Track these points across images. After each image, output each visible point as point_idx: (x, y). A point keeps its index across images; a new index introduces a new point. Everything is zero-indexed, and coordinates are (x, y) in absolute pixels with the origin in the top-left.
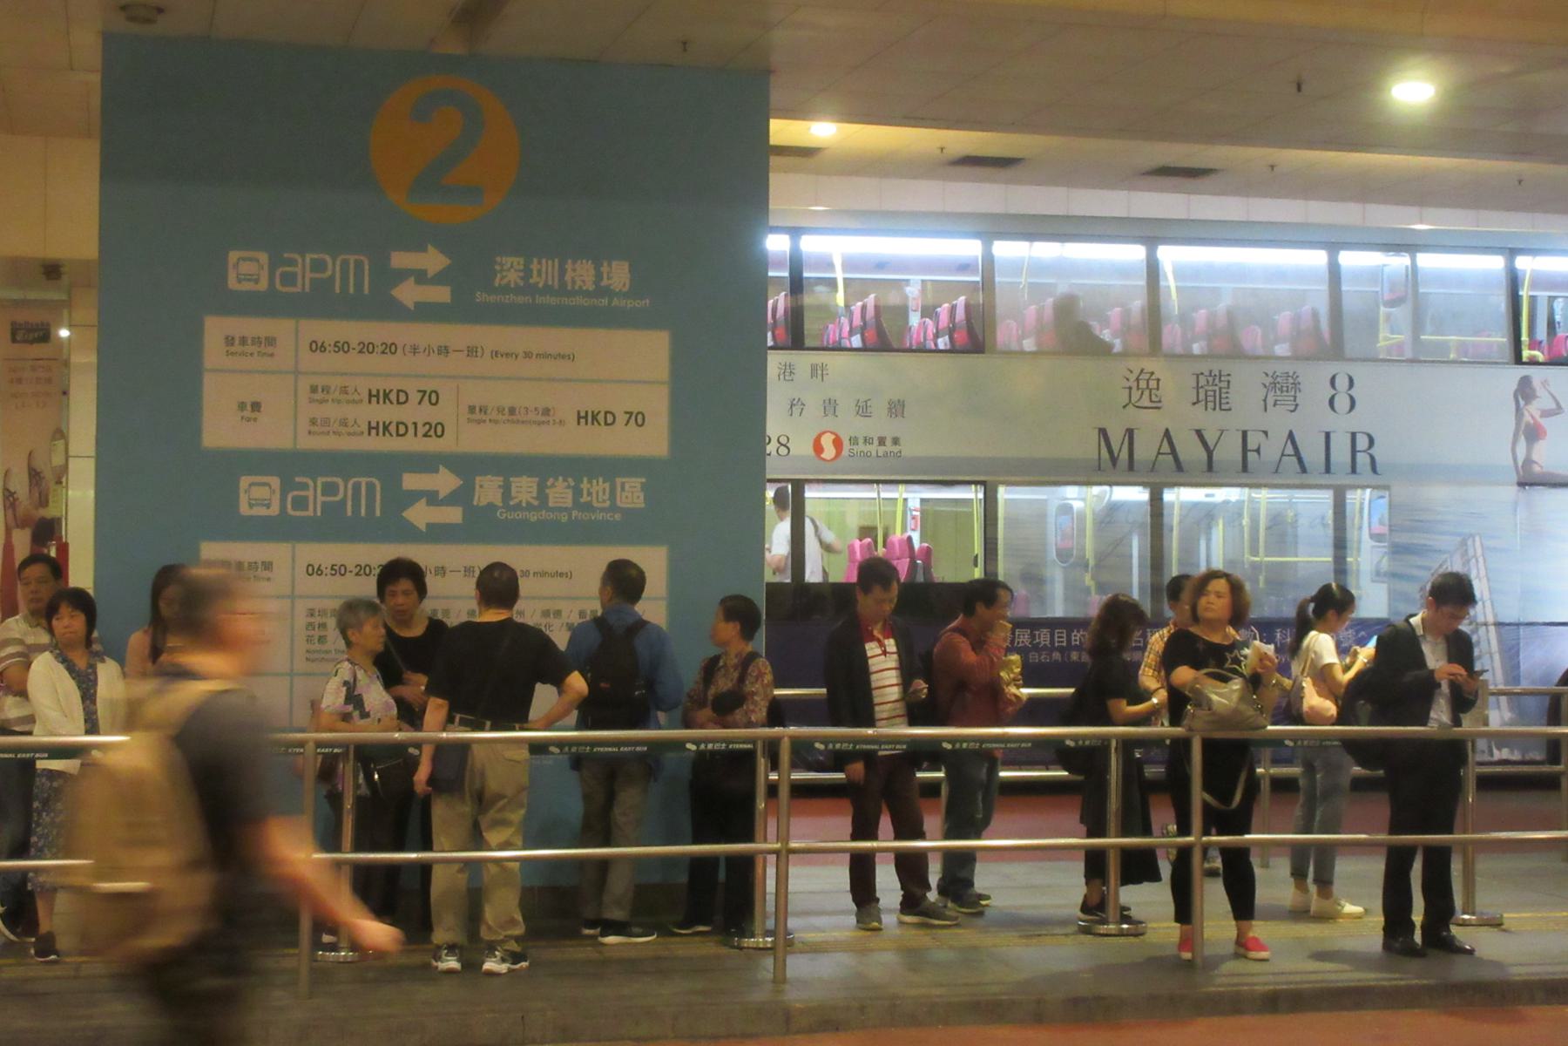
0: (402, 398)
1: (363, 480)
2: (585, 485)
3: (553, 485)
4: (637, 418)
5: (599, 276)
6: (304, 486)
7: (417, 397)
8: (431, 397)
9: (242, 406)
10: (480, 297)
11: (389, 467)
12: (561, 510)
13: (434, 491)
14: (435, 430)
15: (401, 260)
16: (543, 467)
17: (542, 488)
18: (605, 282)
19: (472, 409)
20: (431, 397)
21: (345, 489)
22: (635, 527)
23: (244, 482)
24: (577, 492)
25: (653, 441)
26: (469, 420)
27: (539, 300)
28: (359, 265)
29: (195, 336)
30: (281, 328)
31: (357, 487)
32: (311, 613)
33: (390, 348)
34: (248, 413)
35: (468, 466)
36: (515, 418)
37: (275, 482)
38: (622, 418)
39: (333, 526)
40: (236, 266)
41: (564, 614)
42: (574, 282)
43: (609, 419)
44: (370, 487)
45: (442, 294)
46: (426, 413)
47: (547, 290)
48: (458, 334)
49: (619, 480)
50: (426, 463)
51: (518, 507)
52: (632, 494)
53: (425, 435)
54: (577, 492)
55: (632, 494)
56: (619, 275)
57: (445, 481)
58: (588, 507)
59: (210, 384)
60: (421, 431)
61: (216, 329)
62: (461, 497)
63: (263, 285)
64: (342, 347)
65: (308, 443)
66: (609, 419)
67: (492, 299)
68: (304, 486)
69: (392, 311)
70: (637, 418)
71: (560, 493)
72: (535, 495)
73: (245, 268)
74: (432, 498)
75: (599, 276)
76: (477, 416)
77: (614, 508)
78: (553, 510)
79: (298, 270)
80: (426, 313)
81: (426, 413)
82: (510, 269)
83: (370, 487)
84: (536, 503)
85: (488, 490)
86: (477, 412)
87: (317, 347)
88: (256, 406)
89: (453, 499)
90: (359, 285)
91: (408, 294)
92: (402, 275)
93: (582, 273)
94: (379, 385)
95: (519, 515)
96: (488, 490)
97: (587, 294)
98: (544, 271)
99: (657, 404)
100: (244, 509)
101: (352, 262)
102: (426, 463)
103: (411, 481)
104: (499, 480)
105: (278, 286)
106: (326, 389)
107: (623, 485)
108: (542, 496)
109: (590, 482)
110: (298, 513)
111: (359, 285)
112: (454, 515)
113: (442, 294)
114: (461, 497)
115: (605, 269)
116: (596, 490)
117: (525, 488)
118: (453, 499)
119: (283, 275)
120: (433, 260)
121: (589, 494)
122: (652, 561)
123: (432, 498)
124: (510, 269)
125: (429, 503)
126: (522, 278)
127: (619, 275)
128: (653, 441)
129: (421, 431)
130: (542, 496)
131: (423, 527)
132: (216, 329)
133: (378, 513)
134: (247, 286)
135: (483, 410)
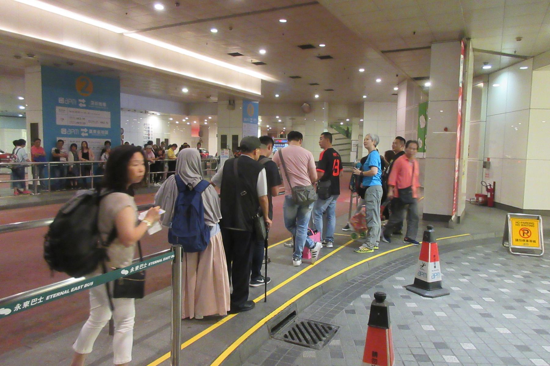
1: (76, 130)
4: (107, 123)
8: (84, 119)
9: (61, 119)
11: (79, 128)
13: (221, 137)
14: (84, 123)
15: (80, 100)
19: (89, 121)
20: (84, 119)
23: (62, 129)
25: (109, 126)
30: (65, 108)
33: (79, 112)
34: (62, 120)
35: (88, 128)
37: (66, 129)
39: (73, 136)
45: (85, 105)
46: (84, 121)
48: (87, 111)
50: (84, 128)
52: (107, 133)
55: (107, 133)
56: (104, 104)
57: (86, 130)
58: (102, 134)
59: (57, 116)
61: (58, 109)
62: (88, 132)
70: (107, 123)
71: (99, 132)
73: (61, 100)
74: (85, 133)
79: (68, 101)
80: (83, 108)
81: (84, 121)
82: (93, 103)
85: (91, 131)
89: (87, 132)
92: (80, 103)
93: (100, 104)
96: (91, 131)
97: (100, 106)
98: (96, 103)
99: (109, 121)
100: (62, 133)
102: (84, 128)
103: (82, 130)
112: (87, 134)
113: (85, 105)
114: (88, 132)
116: (103, 132)
117: (95, 131)
118: (87, 132)
120: (84, 101)
128: (109, 126)
130: (97, 133)
131: (83, 136)
132: (58, 109)
134: (61, 103)
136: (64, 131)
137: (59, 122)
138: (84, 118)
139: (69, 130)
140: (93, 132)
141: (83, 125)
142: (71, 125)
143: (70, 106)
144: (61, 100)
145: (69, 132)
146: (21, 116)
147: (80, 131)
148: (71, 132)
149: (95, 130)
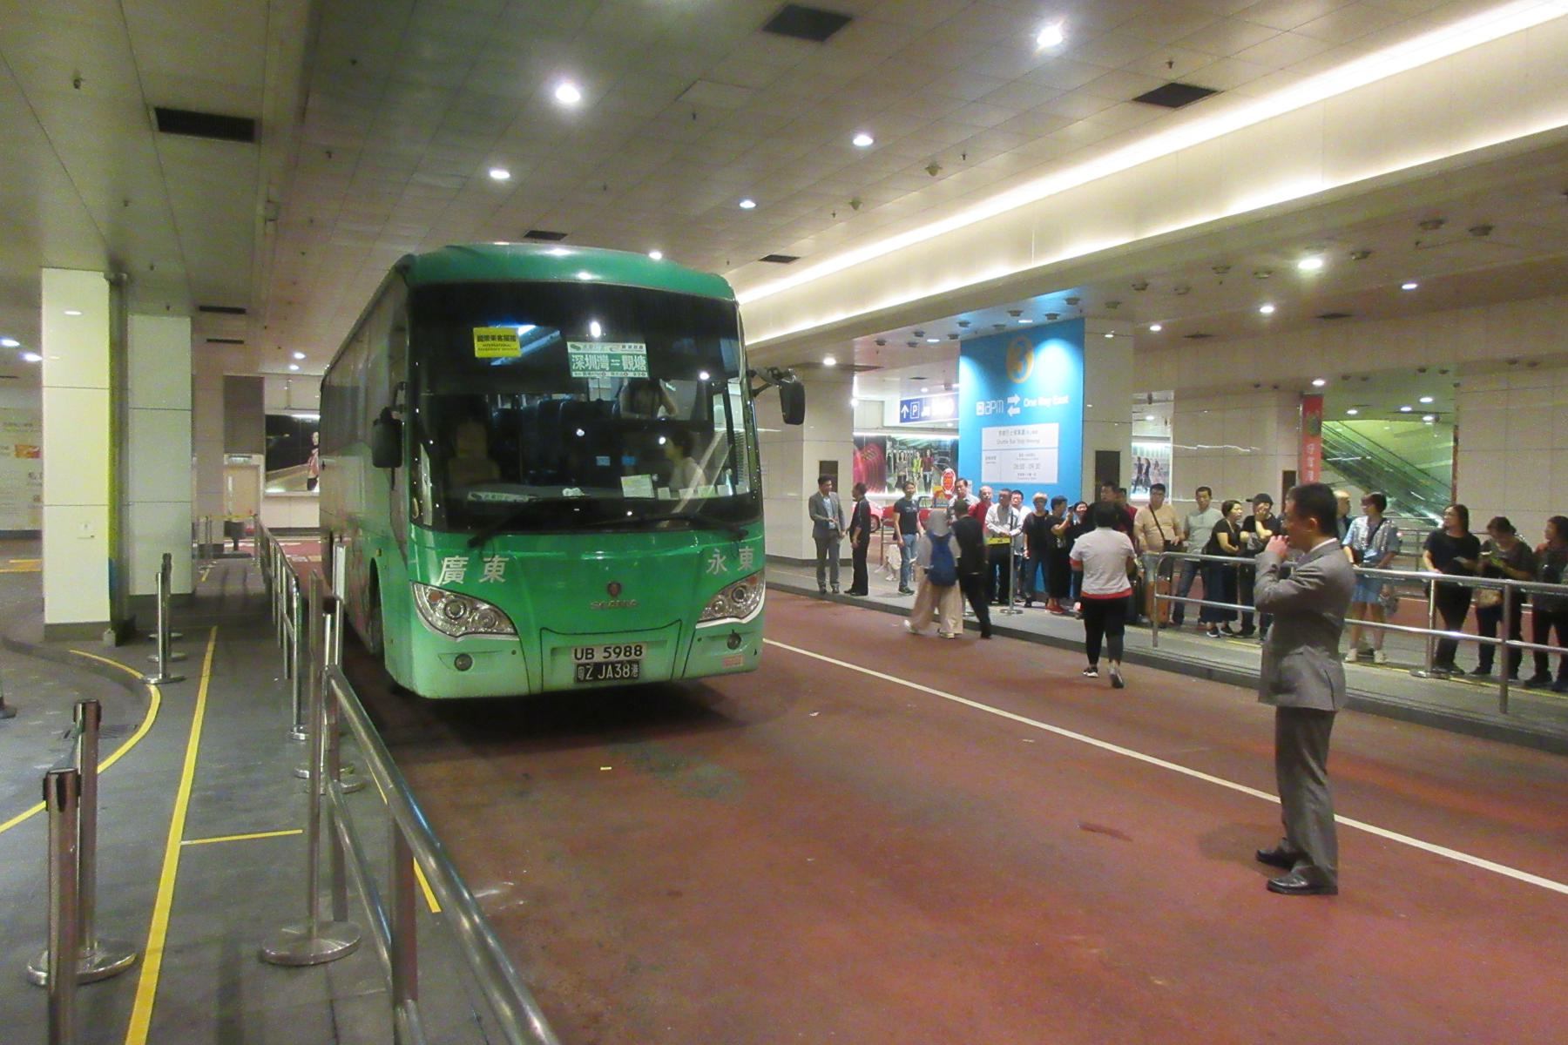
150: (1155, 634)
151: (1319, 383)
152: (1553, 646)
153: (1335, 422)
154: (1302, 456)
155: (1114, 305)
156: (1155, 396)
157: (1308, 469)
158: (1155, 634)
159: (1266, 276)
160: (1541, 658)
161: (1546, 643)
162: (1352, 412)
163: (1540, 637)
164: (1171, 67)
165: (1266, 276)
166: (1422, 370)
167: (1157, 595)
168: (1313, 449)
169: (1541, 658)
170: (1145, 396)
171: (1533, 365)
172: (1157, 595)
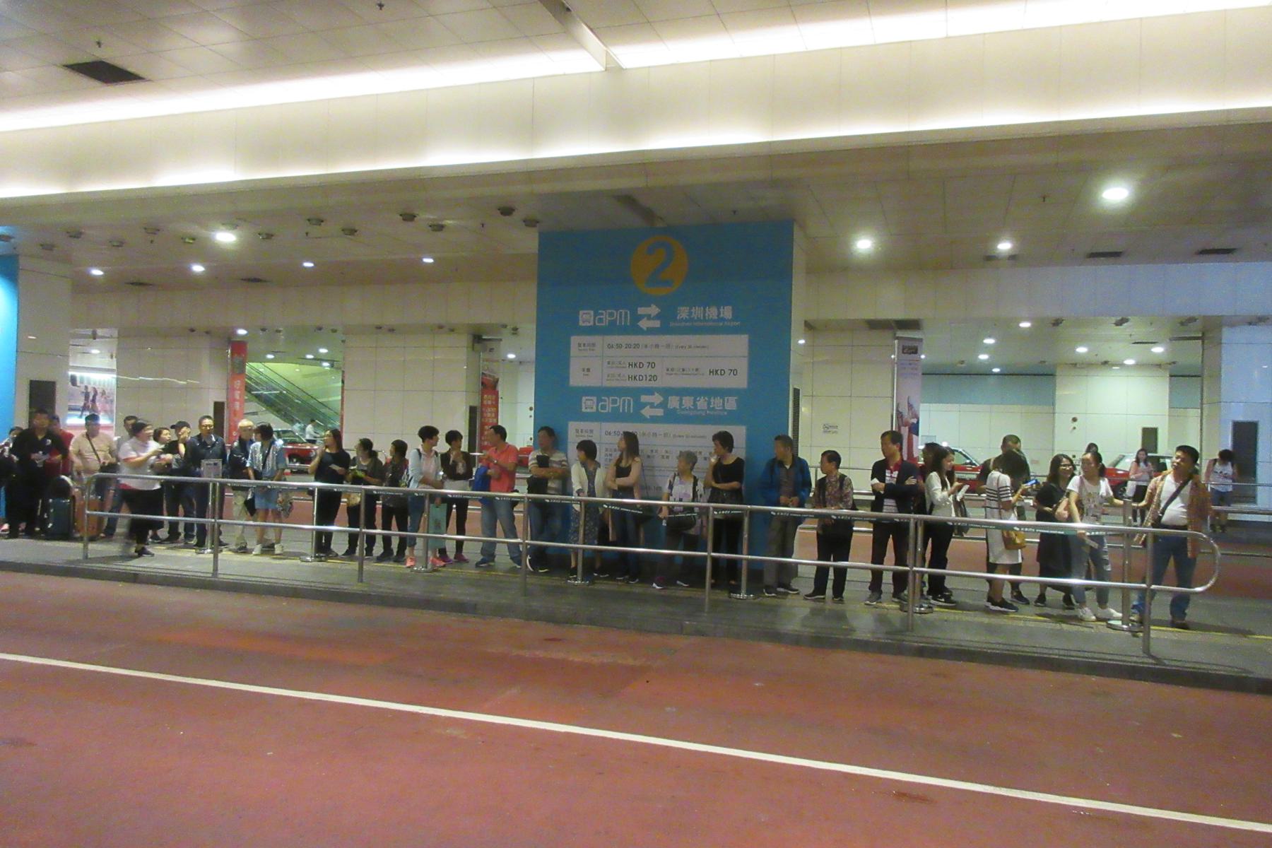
0: (641, 365)
2: (712, 400)
3: (699, 401)
4: (734, 372)
5: (719, 313)
6: (605, 401)
7: (646, 365)
10: (672, 324)
11: (635, 393)
12: (703, 410)
14: (654, 378)
15: (641, 311)
16: (696, 393)
17: (695, 401)
18: (722, 315)
19: (668, 370)
20: (652, 365)
21: (620, 402)
22: (733, 418)
24: (709, 404)
25: (741, 381)
26: (667, 374)
27: (696, 324)
28: (626, 314)
29: (567, 346)
30: (597, 339)
31: (624, 401)
32: (607, 450)
33: (637, 346)
35: (667, 392)
36: (685, 372)
38: (727, 372)
39: (615, 416)
40: (582, 317)
41: (703, 454)
42: (709, 315)
43: (722, 372)
44: (629, 401)
45: (657, 324)
46: (650, 371)
47: (699, 320)
49: (726, 398)
50: (650, 391)
51: (685, 409)
52: (731, 404)
53: (650, 380)
54: (709, 404)
55: (731, 404)
56: (727, 312)
57: (657, 398)
60: (648, 378)
61: (575, 340)
62: (663, 405)
63: (592, 323)
64: (619, 346)
65: (608, 384)
66: (722, 372)
67: (677, 324)
68: (605, 401)
69: (638, 331)
70: (734, 372)
71: (702, 403)
72: (692, 404)
74: (652, 406)
75: (719, 313)
76: (670, 372)
77: (724, 410)
78: (700, 410)
80: (651, 331)
81: (650, 371)
82: (683, 312)
83: (629, 401)
84: (692, 407)
85: (673, 402)
86: (670, 371)
87: (610, 346)
88: (588, 370)
90: (626, 322)
91: (644, 324)
93: (712, 312)
94: (632, 361)
95: (686, 412)
96: (673, 402)
97: (714, 321)
98: (697, 312)
99: (743, 366)
100: (584, 410)
101: (623, 313)
102: (650, 391)
103: (644, 398)
104: (678, 398)
105: (597, 324)
106: (613, 363)
107: (728, 400)
108: (695, 405)
109: (714, 398)
110: (602, 411)
111: (626, 322)
113: (657, 324)
114: (663, 405)
115: (722, 310)
116: (717, 402)
117: (688, 401)
119: (600, 318)
120: (654, 310)
121: (714, 403)
122: (739, 433)
123: (652, 406)
124: (683, 312)
125: (651, 407)
126: (688, 315)
127: (727, 312)
128: (741, 381)
129: (648, 378)
130: (695, 405)
132: (575, 340)
133: (632, 411)
135: (672, 370)
136: (588, 404)
137: (577, 379)
138: (651, 361)
139: (605, 401)
140: (681, 404)
141: (652, 384)
142: (614, 384)
143: (612, 329)
144: (586, 317)
145: (603, 407)
146: (996, 370)
147: (637, 401)
148: (611, 406)
149: (688, 398)
150: (85, 547)
151: (242, 332)
152: (394, 532)
153: (259, 364)
154: (230, 390)
155: (48, 247)
156: (100, 332)
157: (235, 400)
158: (85, 547)
159: (191, 241)
160: (387, 540)
161: (390, 530)
162: (270, 356)
163: (386, 526)
164: (100, 47)
165: (191, 241)
166: (320, 329)
167: (88, 512)
168: (239, 384)
169: (387, 540)
170: (89, 331)
171: (392, 330)
172: (88, 512)
